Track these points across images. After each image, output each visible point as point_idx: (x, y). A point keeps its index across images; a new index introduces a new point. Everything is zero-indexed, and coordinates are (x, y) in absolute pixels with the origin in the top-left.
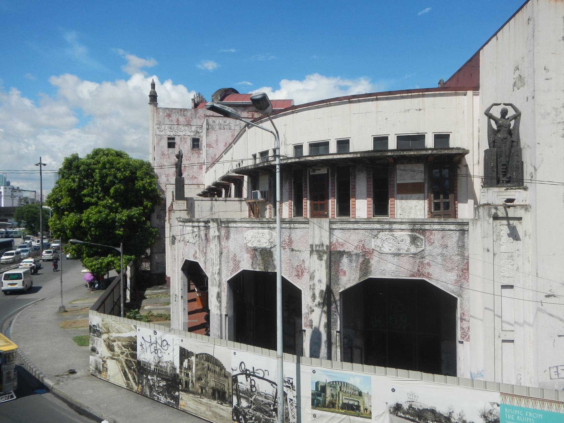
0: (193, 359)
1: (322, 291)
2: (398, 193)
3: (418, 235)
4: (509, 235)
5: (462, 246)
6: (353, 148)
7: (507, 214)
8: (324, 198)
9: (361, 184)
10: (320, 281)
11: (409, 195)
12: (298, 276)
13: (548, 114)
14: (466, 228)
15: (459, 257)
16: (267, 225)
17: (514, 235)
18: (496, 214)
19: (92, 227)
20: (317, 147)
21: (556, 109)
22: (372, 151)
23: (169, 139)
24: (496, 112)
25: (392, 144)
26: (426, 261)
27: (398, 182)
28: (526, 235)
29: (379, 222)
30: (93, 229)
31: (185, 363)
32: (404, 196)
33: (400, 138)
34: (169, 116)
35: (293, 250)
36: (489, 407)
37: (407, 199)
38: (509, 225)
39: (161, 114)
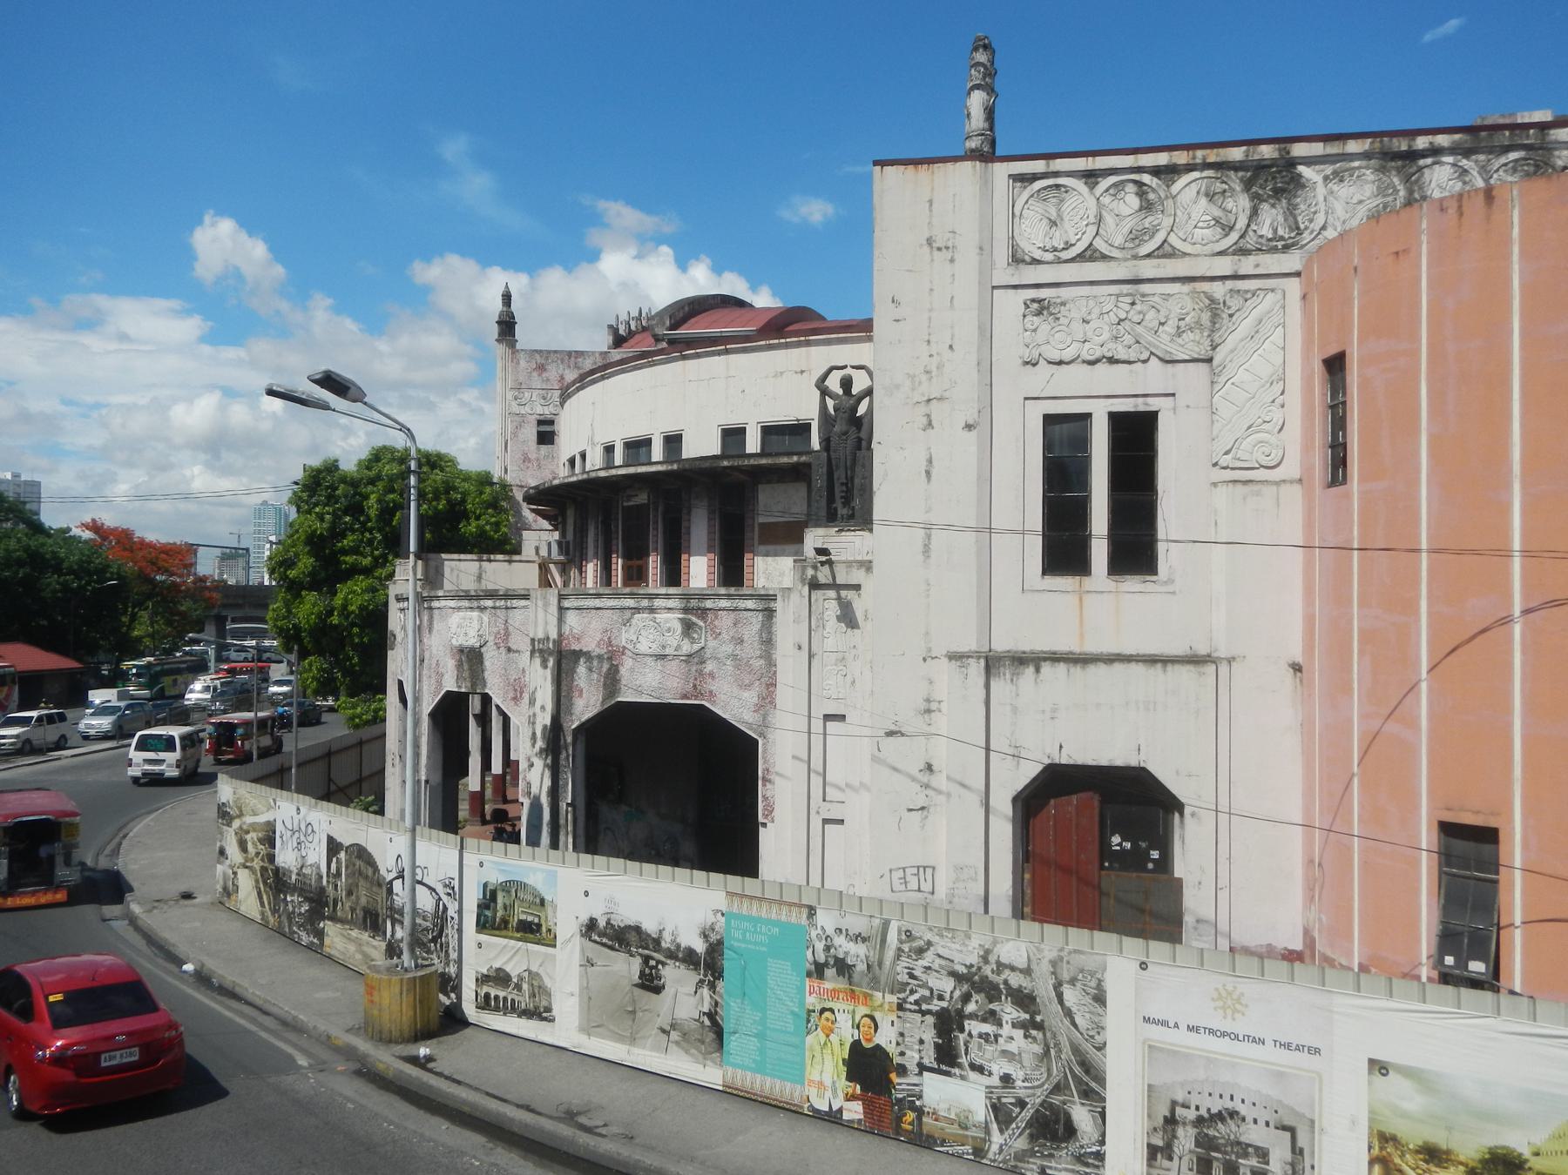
0: (342, 855)
1: (545, 727)
2: (763, 542)
3: (694, 619)
4: (839, 619)
5: (768, 641)
6: (690, 450)
7: (834, 578)
8: (644, 554)
9: (700, 527)
10: (543, 708)
11: (779, 547)
12: (515, 699)
13: (897, 387)
14: (772, 605)
15: (762, 662)
16: (475, 604)
17: (848, 618)
18: (814, 577)
19: (353, 625)
20: (637, 447)
21: (912, 377)
22: (715, 457)
23: (540, 423)
24: (834, 383)
25: (753, 444)
26: (707, 670)
27: (761, 520)
28: (866, 618)
29: (632, 595)
30: (355, 630)
31: (334, 866)
32: (771, 548)
33: (768, 431)
34: (541, 368)
35: (509, 650)
36: (711, 919)
37: (776, 555)
38: (839, 598)
39: (523, 363)
